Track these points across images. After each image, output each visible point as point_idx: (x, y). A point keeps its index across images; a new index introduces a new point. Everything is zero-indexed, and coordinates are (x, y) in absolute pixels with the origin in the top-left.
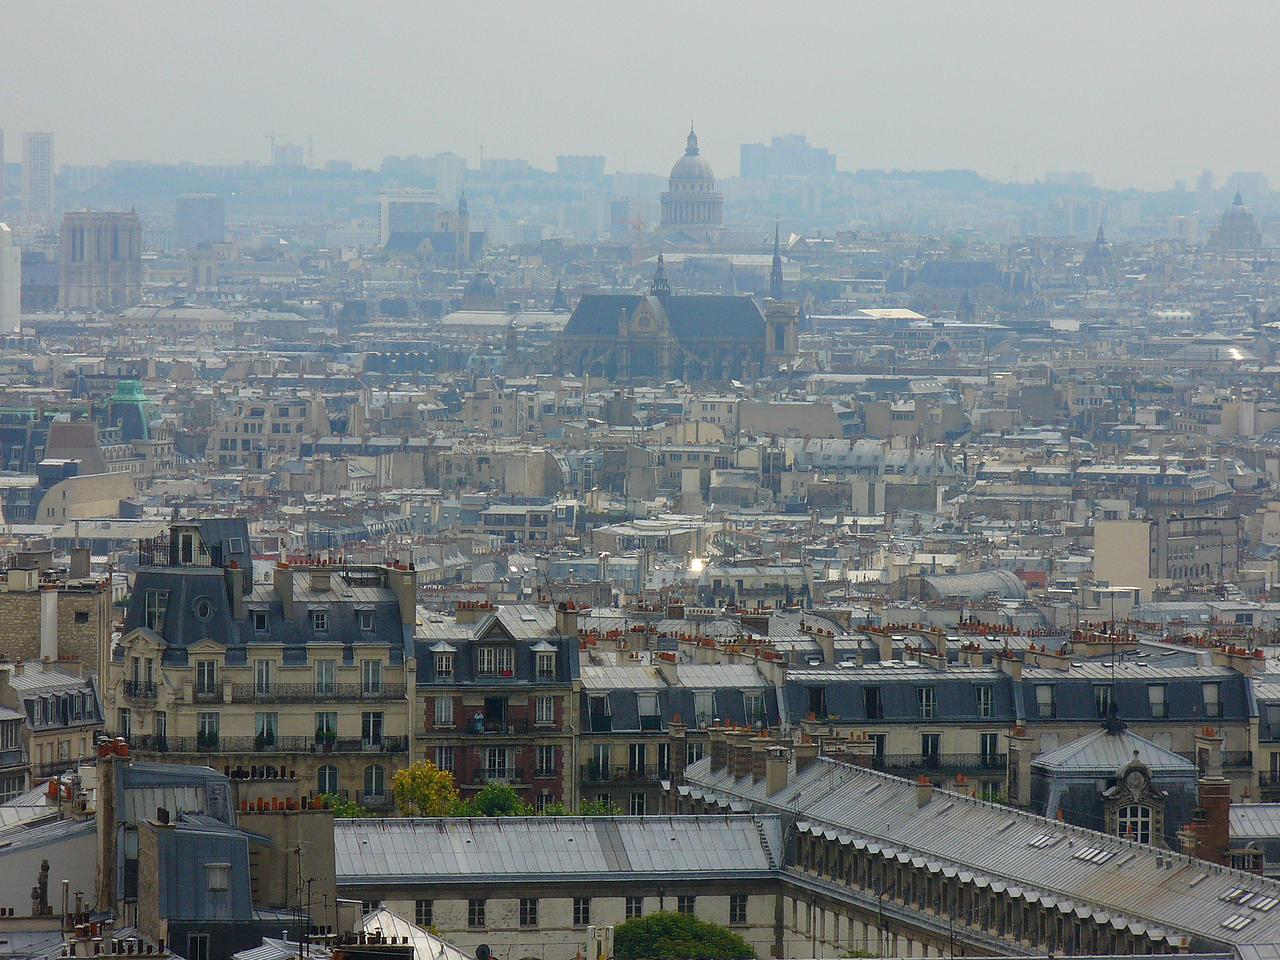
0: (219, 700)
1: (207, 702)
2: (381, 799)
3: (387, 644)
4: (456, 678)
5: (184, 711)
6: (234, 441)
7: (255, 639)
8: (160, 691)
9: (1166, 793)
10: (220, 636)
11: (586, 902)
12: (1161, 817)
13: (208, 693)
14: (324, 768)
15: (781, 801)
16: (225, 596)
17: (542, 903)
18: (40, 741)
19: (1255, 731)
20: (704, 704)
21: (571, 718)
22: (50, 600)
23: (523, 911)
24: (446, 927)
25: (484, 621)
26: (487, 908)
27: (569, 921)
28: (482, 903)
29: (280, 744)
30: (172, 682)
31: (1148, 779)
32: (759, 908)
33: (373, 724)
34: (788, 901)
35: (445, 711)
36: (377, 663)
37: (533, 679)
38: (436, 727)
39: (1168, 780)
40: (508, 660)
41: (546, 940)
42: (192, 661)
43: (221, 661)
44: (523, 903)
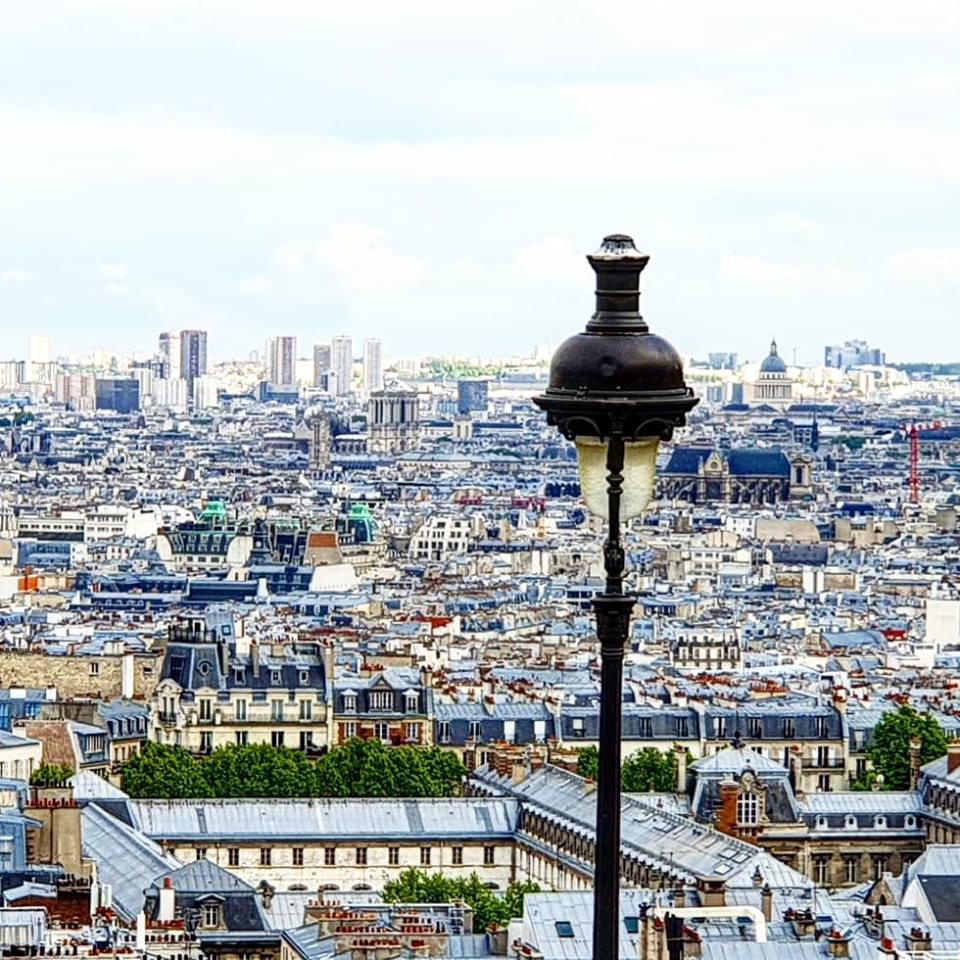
4: (358, 711)
5: (192, 729)
6: (427, 544)
7: (235, 687)
8: (178, 718)
10: (214, 685)
12: (764, 800)
13: (207, 718)
15: (518, 790)
16: (217, 661)
17: (370, 851)
20: (509, 729)
21: (427, 736)
22: (129, 659)
23: (358, 856)
30: (182, 711)
31: (755, 777)
32: (502, 854)
34: (518, 850)
36: (281, 701)
37: (404, 712)
42: (197, 700)
43: (214, 700)
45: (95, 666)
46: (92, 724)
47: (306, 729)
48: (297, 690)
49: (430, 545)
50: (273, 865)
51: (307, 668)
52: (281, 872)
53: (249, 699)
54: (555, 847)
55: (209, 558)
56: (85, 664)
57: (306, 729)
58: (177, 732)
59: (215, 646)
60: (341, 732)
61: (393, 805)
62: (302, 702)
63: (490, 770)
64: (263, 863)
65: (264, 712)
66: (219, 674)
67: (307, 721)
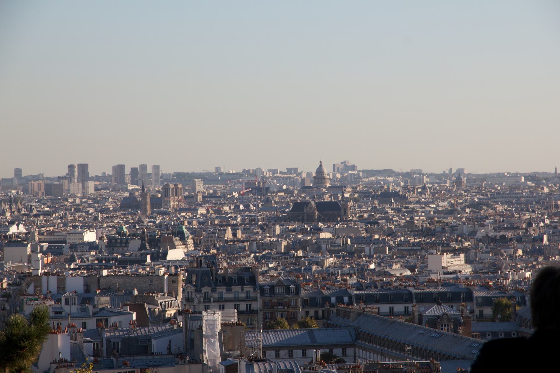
0: (210, 301)
5: (201, 304)
6: (208, 240)
7: (219, 286)
8: (195, 299)
9: (453, 320)
10: (210, 286)
11: (305, 351)
17: (294, 351)
19: (475, 304)
23: (289, 353)
26: (280, 353)
28: (279, 351)
32: (350, 351)
33: (249, 307)
34: (357, 350)
39: (453, 317)
40: (283, 289)
42: (203, 292)
43: (210, 292)
44: (289, 351)
47: (249, 303)
48: (244, 287)
49: (209, 241)
53: (224, 291)
54: (378, 347)
55: (121, 249)
57: (249, 303)
58: (194, 306)
59: (209, 269)
63: (337, 316)
65: (231, 295)
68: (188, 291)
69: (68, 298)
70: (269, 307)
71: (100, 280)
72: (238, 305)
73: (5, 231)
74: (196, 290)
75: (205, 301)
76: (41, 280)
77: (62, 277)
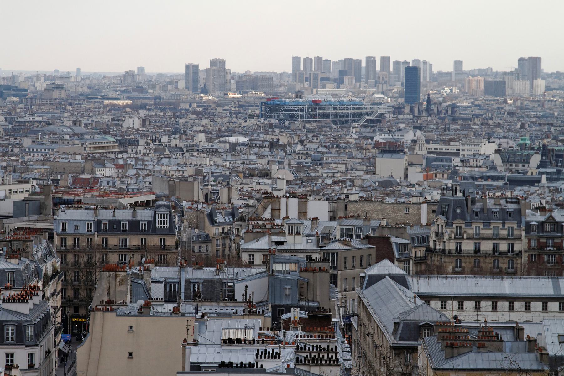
0: (463, 238)
1: (458, 239)
2: (512, 270)
3: (516, 222)
4: (538, 233)
5: (451, 241)
7: (475, 219)
8: (445, 234)
10: (463, 217)
11: (546, 303)
13: (459, 236)
14: (495, 260)
16: (465, 206)
18: (416, 250)
22: (425, 207)
23: (526, 306)
24: (501, 310)
25: (548, 214)
27: (558, 310)
28: (513, 303)
29: (481, 252)
30: (447, 232)
35: (534, 244)
38: (531, 248)
41: (533, 315)
42: (454, 226)
43: (463, 226)
44: (526, 303)
45: (408, 209)
46: (403, 238)
50: (481, 309)
51: (512, 210)
52: (486, 313)
53: (481, 226)
55: (520, 165)
56: (402, 208)
58: (445, 242)
59: (464, 198)
60: (529, 243)
61: (546, 280)
62: (509, 227)
64: (476, 308)
65: (489, 232)
66: (466, 213)
67: (512, 238)
68: (438, 223)
69: (292, 227)
70: (536, 248)
71: (348, 206)
72: (497, 243)
73: (400, 137)
74: (446, 223)
75: (457, 236)
76: (279, 202)
77: (304, 200)
